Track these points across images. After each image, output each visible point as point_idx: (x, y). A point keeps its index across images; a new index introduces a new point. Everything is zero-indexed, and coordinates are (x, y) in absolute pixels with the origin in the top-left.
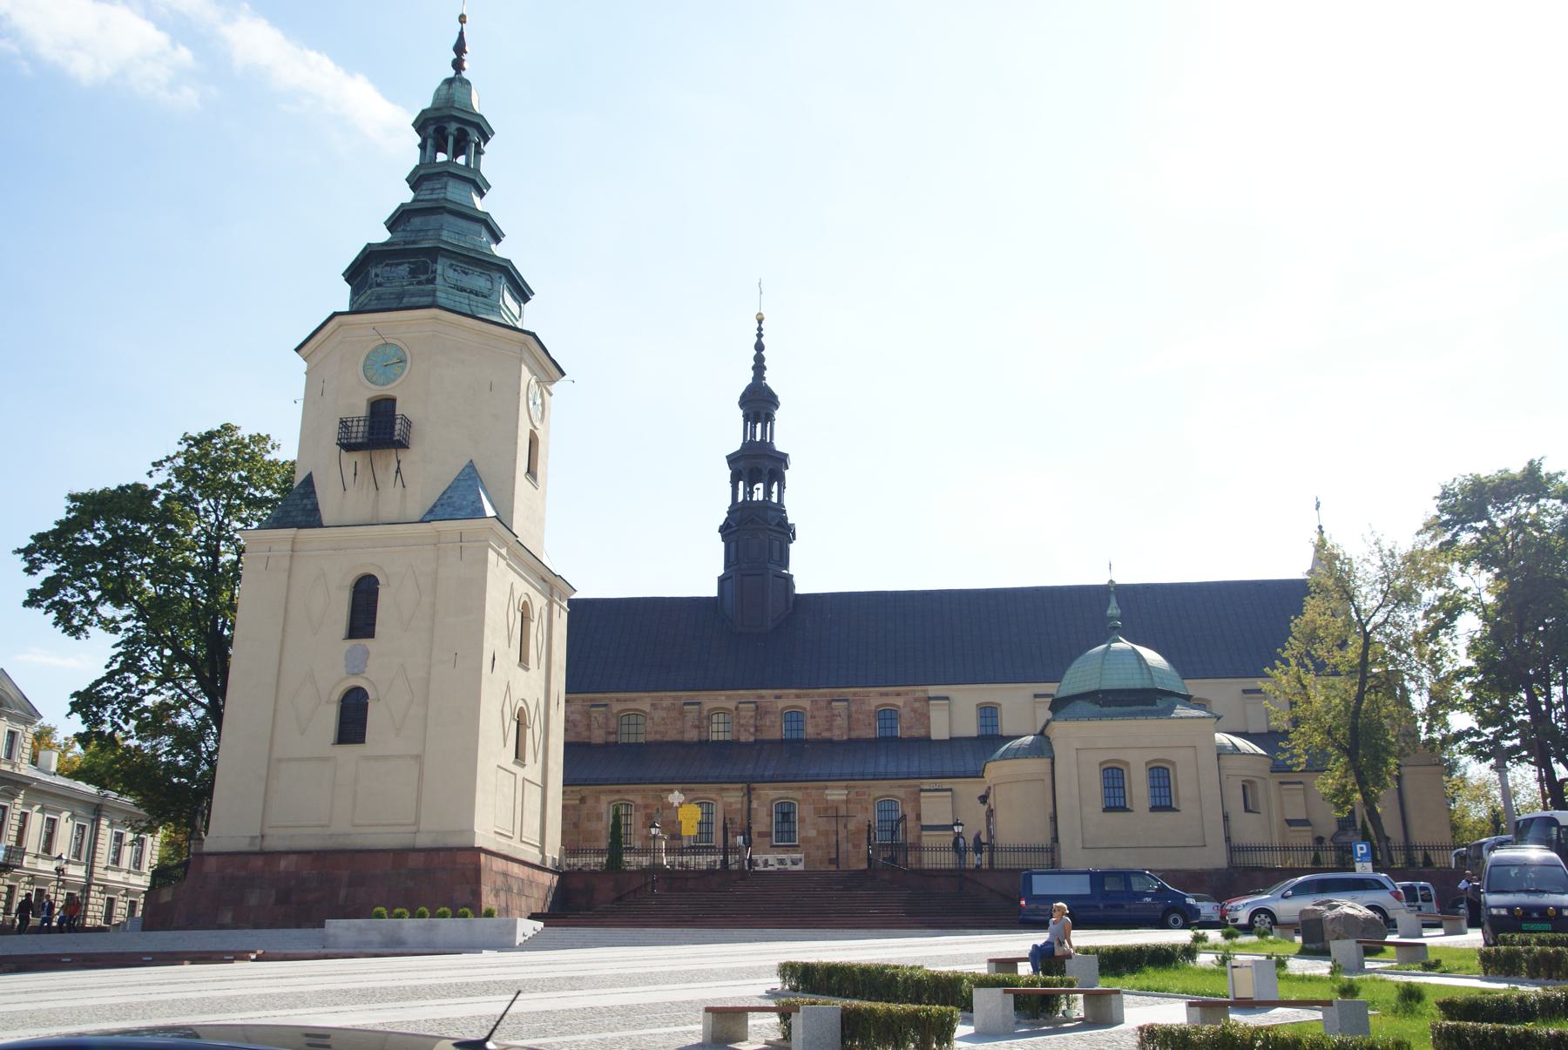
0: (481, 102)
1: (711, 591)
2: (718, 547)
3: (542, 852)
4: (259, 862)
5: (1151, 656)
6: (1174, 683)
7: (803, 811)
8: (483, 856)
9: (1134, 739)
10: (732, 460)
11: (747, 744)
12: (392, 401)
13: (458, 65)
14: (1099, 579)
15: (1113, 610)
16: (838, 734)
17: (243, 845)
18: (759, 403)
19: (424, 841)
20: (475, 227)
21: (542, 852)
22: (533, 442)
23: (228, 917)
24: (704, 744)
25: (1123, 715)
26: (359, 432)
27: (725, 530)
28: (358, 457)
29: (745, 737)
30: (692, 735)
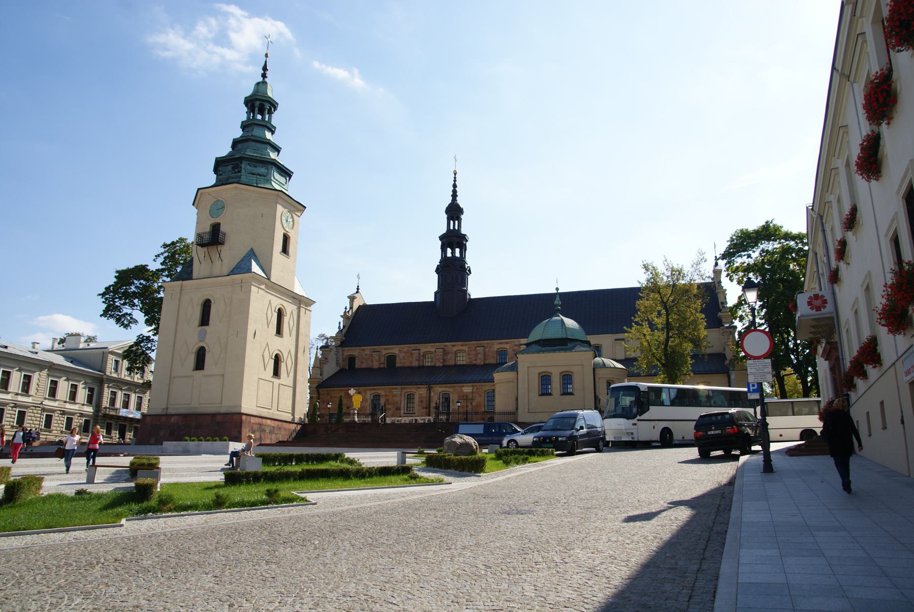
0: (272, 92)
1: (433, 300)
2: (435, 277)
3: (293, 414)
4: (164, 419)
5: (570, 323)
6: (582, 336)
7: (453, 397)
8: (244, 417)
9: (555, 362)
10: (441, 238)
11: (439, 367)
12: (219, 224)
13: (264, 76)
14: (548, 289)
15: (557, 301)
16: (479, 362)
17: (160, 412)
18: (454, 212)
19: (223, 410)
20: (264, 146)
21: (293, 414)
22: (286, 239)
23: (153, 440)
24: (421, 368)
25: (549, 351)
26: (207, 238)
27: (438, 270)
28: (205, 249)
29: (439, 364)
30: (415, 364)
